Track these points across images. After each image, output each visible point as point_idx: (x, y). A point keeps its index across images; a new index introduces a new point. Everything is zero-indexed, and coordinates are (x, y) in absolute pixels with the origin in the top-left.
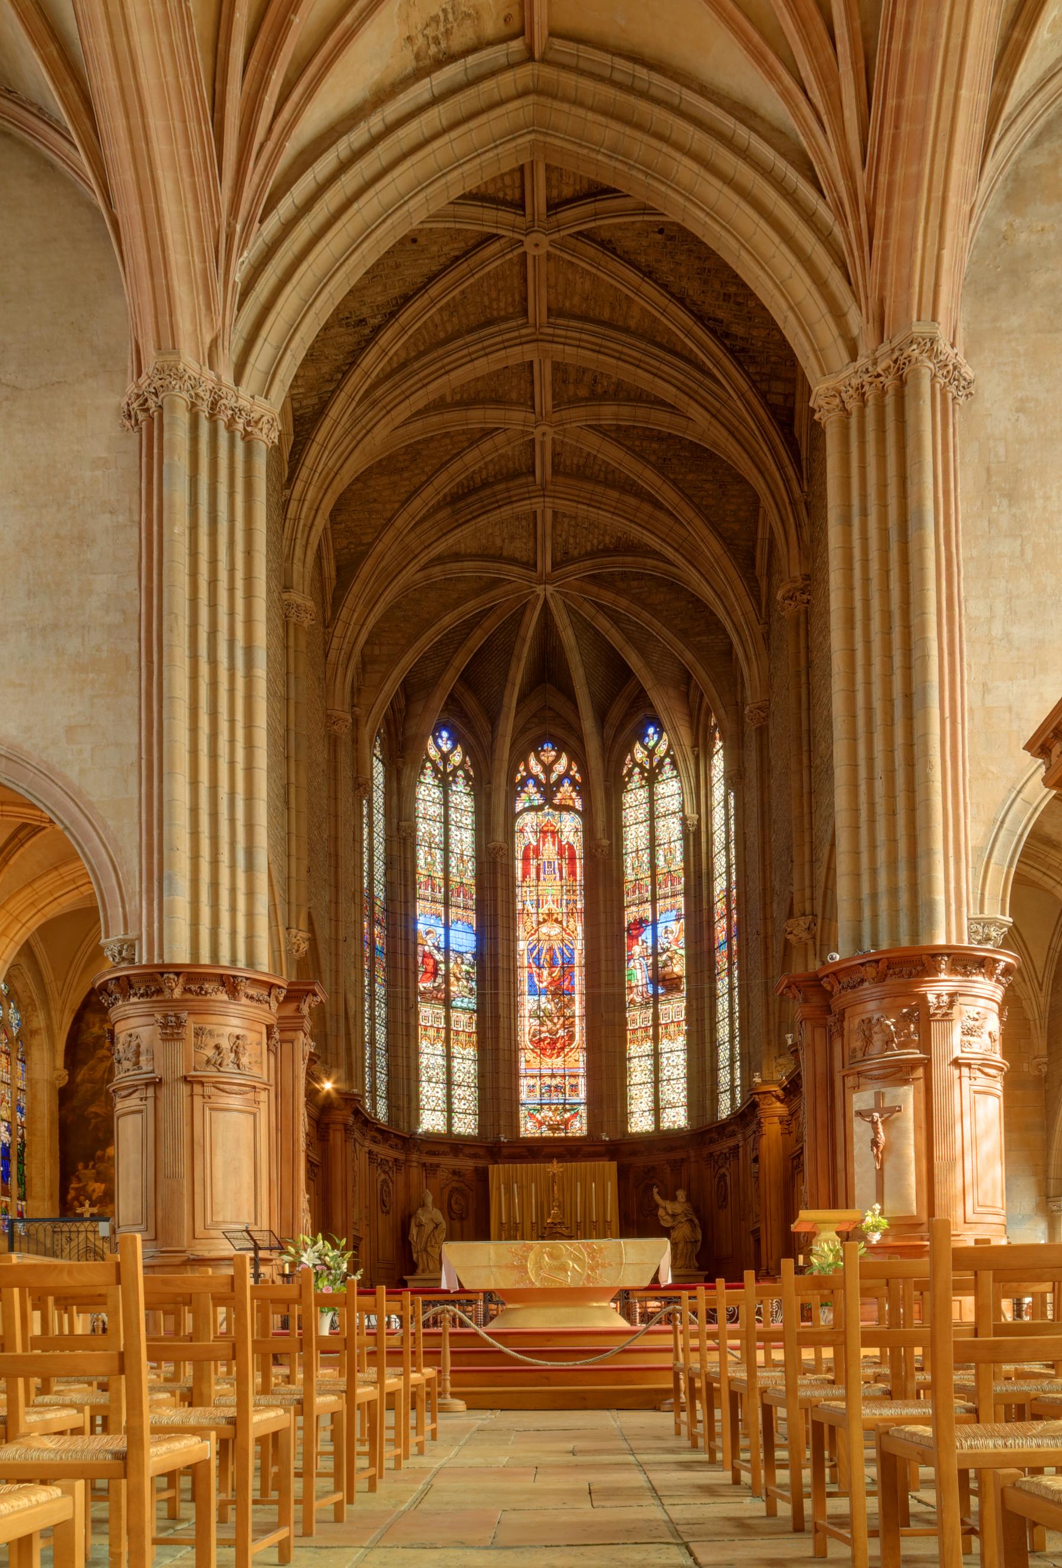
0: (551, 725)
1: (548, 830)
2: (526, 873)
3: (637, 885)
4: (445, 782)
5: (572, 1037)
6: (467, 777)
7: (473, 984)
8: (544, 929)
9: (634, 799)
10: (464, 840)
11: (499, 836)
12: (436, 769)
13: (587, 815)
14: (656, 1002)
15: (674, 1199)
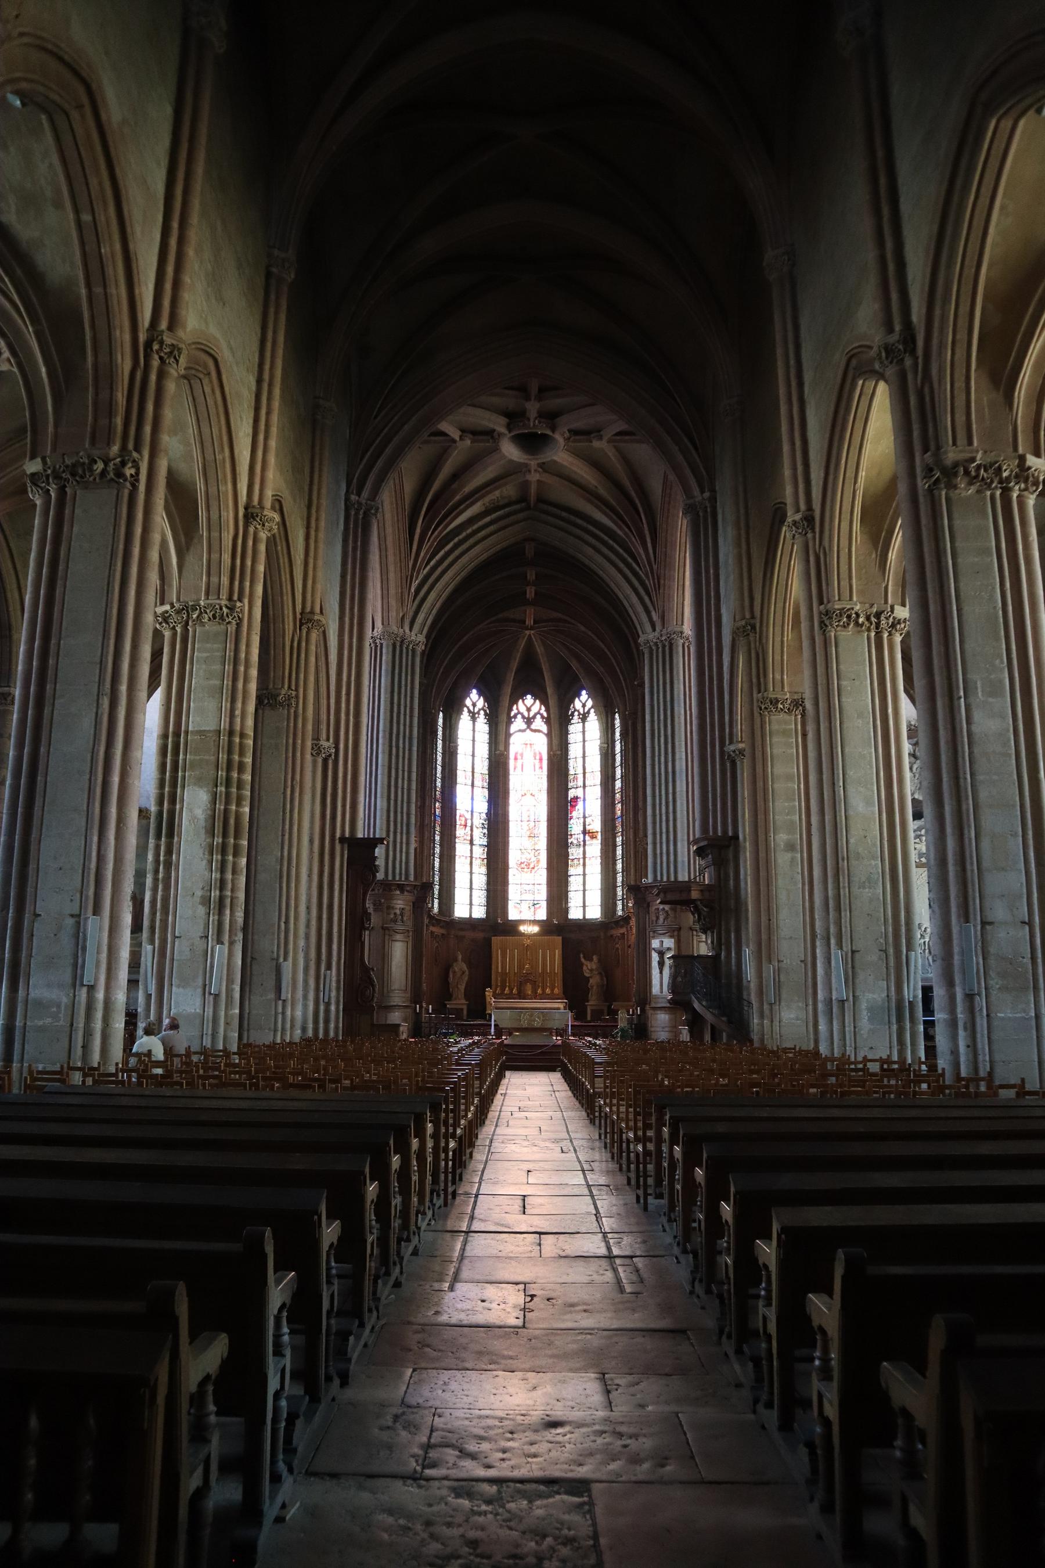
1: (528, 744)
4: (474, 717)
5: (538, 861)
6: (486, 714)
7: (485, 831)
9: (575, 729)
11: (502, 748)
12: (469, 711)
13: (549, 735)
14: (584, 845)
15: (591, 960)
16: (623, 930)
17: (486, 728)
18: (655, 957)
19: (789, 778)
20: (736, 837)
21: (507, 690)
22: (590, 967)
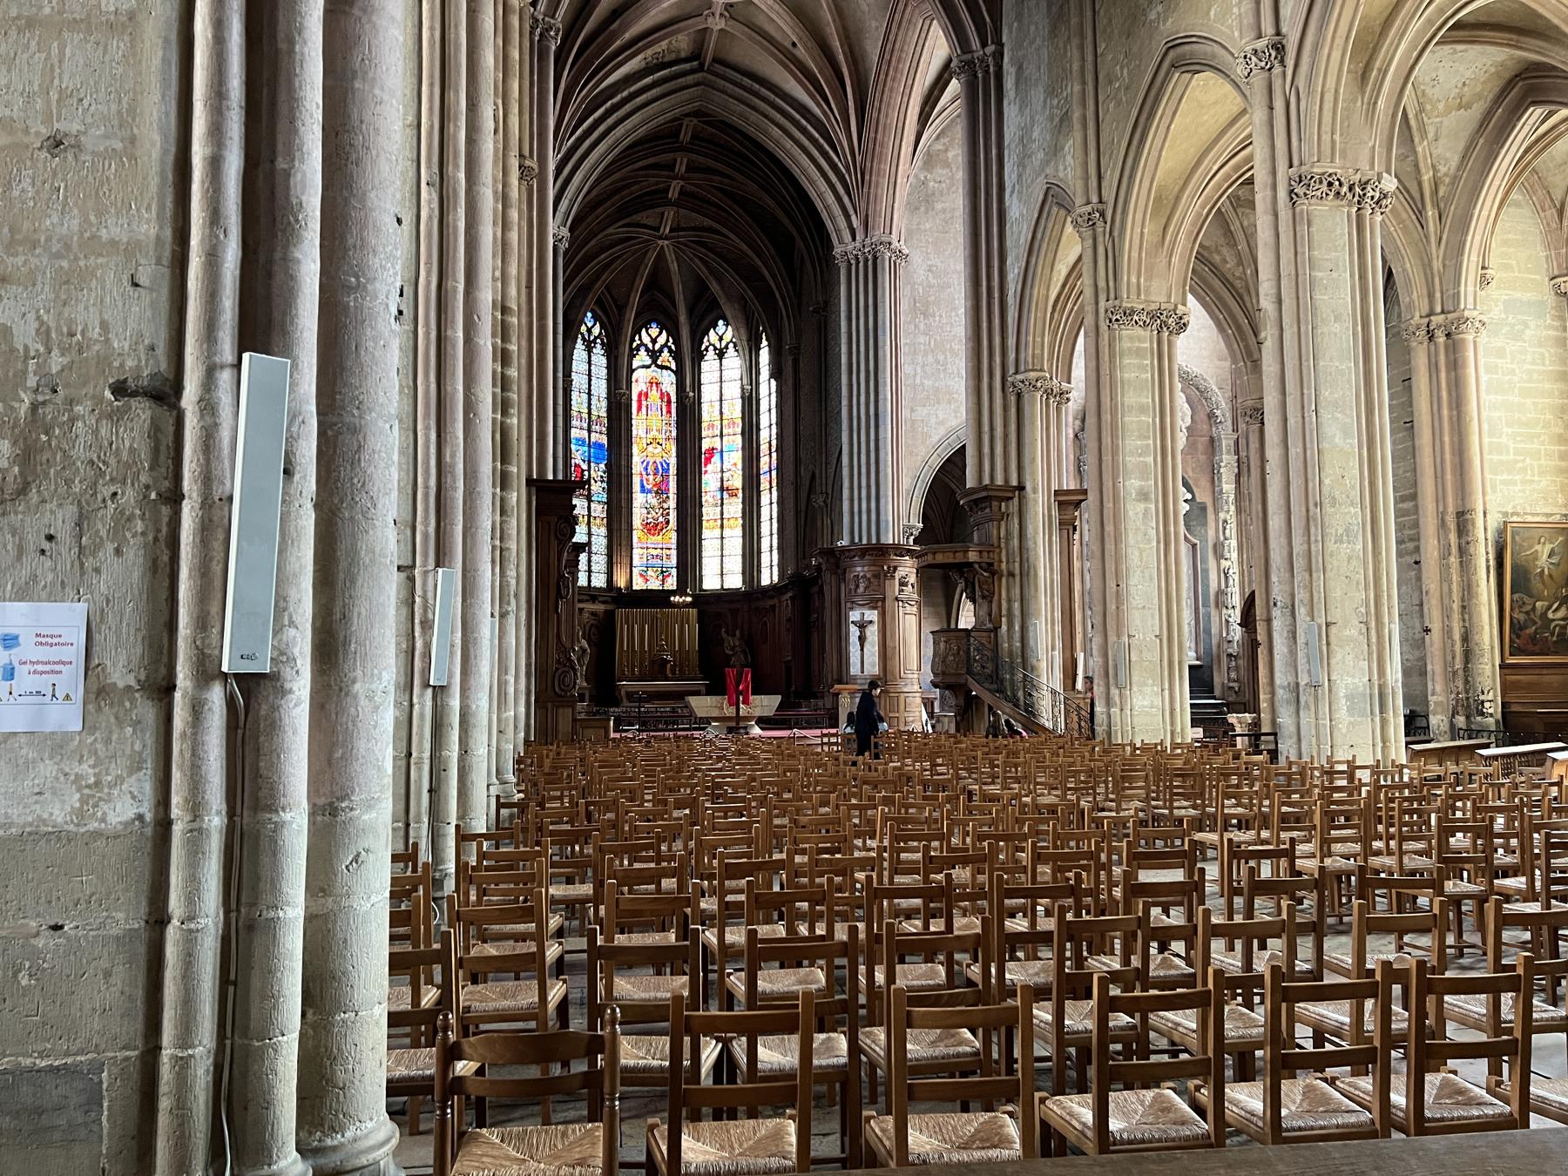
0: (657, 311)
1: (651, 379)
2: (639, 408)
3: (711, 426)
8: (650, 448)
9: (709, 365)
10: (600, 388)
13: (679, 373)
16: (771, 602)
17: (604, 361)
18: (854, 632)
19: (1142, 409)
20: (1021, 488)
21: (631, 315)
22: (732, 642)
